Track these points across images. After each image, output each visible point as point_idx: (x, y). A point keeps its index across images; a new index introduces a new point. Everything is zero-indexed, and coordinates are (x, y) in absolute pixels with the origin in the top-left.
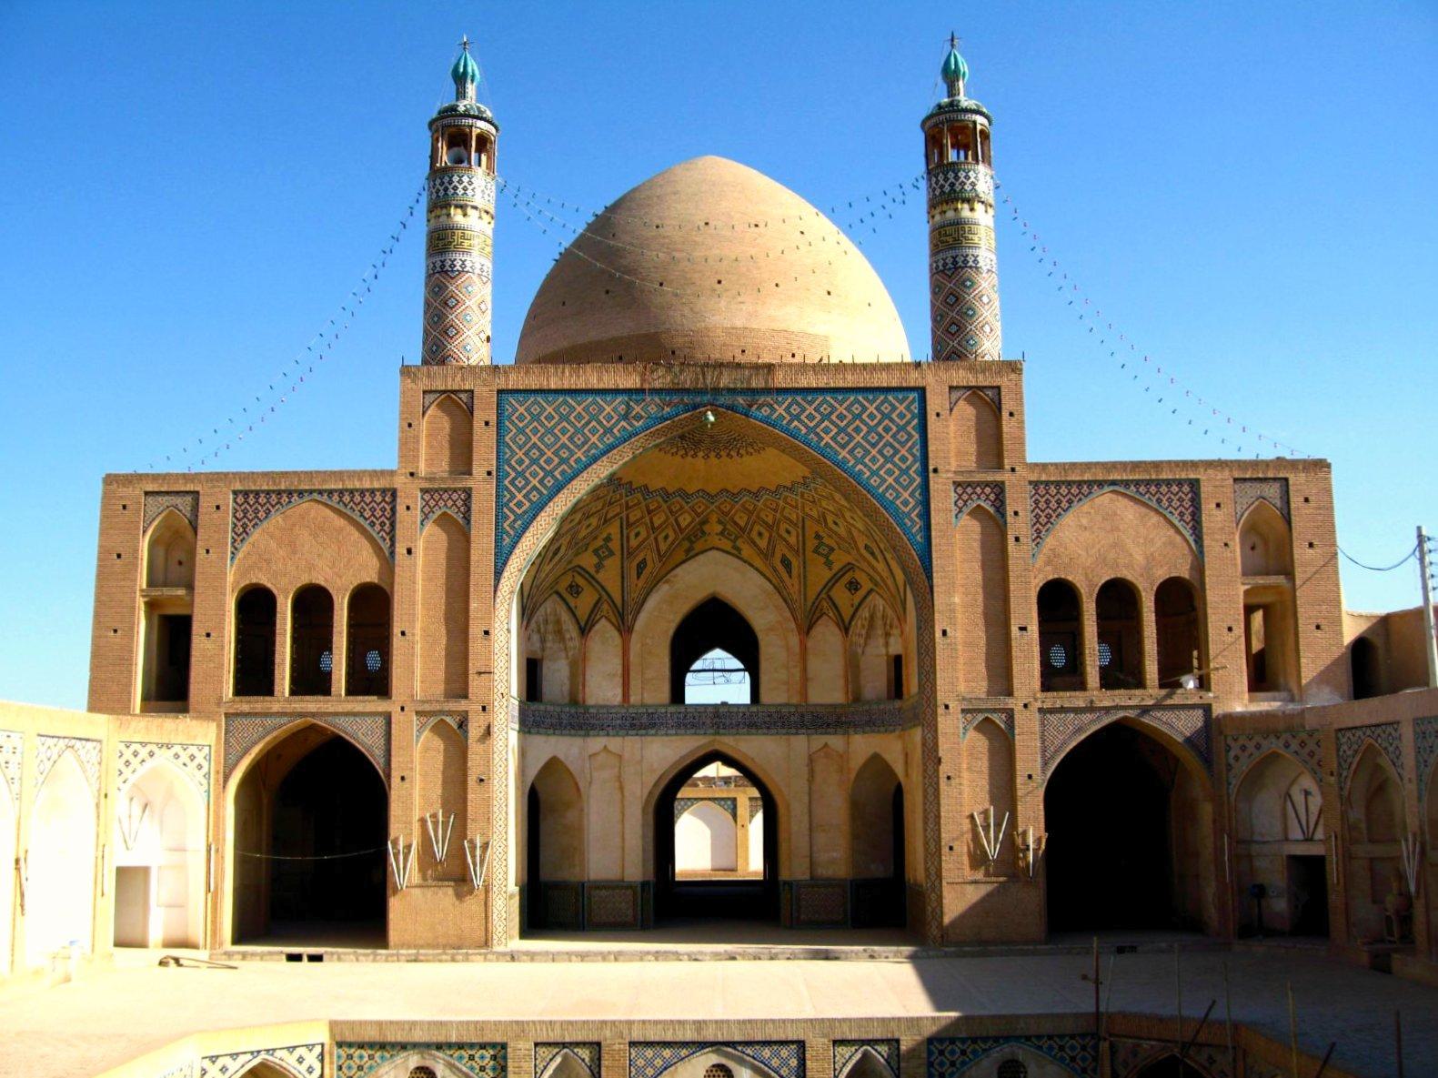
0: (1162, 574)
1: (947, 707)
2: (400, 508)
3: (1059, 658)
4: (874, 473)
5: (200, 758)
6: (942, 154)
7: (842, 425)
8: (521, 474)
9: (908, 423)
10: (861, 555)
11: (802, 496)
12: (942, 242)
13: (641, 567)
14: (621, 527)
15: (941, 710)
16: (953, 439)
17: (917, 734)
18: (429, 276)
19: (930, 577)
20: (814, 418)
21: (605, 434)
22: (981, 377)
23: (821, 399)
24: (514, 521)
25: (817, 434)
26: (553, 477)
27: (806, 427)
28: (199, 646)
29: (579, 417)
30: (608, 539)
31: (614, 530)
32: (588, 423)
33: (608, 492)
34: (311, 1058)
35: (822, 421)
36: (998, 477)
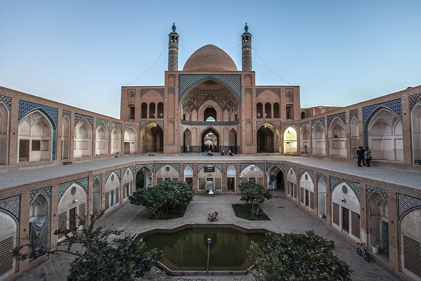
2: (165, 92)
3: (259, 115)
5: (136, 127)
6: (244, 41)
8: (182, 87)
13: (200, 101)
15: (242, 121)
17: (239, 125)
19: (241, 102)
28: (136, 111)
30: (195, 97)
31: (196, 96)
34: (152, 166)
36: (251, 88)
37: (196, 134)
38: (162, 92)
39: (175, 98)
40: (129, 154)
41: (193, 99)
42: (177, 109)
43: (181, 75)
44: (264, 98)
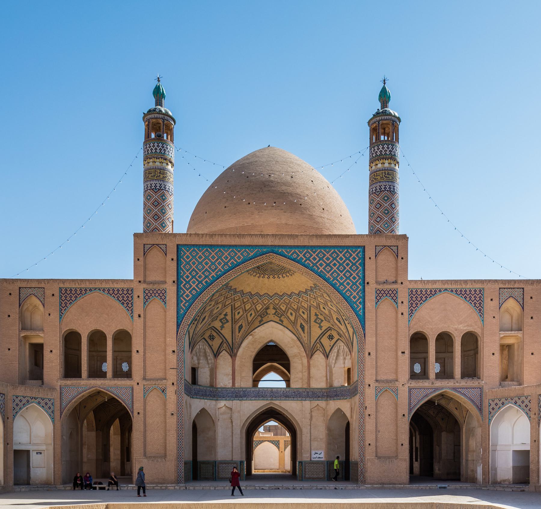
0: (464, 328)
1: (369, 385)
2: (135, 297)
4: (342, 284)
7: (328, 262)
9: (357, 262)
10: (335, 322)
11: (310, 296)
12: (375, 179)
14: (232, 309)
16: (376, 270)
18: (145, 191)
19: (364, 329)
20: (316, 259)
21: (224, 265)
22: (390, 241)
23: (319, 250)
24: (185, 303)
25: (317, 267)
26: (202, 284)
27: (313, 263)
29: (213, 257)
32: (217, 260)
33: (226, 292)
35: (319, 261)
36: (394, 286)
37: (230, 426)
38: (125, 299)
39: (168, 319)
40: (28, 484)
41: (221, 320)
42: (174, 351)
43: (183, 248)
44: (433, 320)
